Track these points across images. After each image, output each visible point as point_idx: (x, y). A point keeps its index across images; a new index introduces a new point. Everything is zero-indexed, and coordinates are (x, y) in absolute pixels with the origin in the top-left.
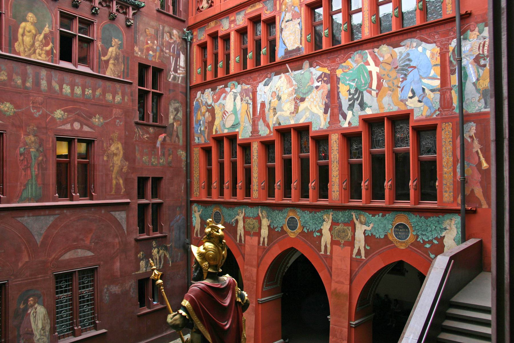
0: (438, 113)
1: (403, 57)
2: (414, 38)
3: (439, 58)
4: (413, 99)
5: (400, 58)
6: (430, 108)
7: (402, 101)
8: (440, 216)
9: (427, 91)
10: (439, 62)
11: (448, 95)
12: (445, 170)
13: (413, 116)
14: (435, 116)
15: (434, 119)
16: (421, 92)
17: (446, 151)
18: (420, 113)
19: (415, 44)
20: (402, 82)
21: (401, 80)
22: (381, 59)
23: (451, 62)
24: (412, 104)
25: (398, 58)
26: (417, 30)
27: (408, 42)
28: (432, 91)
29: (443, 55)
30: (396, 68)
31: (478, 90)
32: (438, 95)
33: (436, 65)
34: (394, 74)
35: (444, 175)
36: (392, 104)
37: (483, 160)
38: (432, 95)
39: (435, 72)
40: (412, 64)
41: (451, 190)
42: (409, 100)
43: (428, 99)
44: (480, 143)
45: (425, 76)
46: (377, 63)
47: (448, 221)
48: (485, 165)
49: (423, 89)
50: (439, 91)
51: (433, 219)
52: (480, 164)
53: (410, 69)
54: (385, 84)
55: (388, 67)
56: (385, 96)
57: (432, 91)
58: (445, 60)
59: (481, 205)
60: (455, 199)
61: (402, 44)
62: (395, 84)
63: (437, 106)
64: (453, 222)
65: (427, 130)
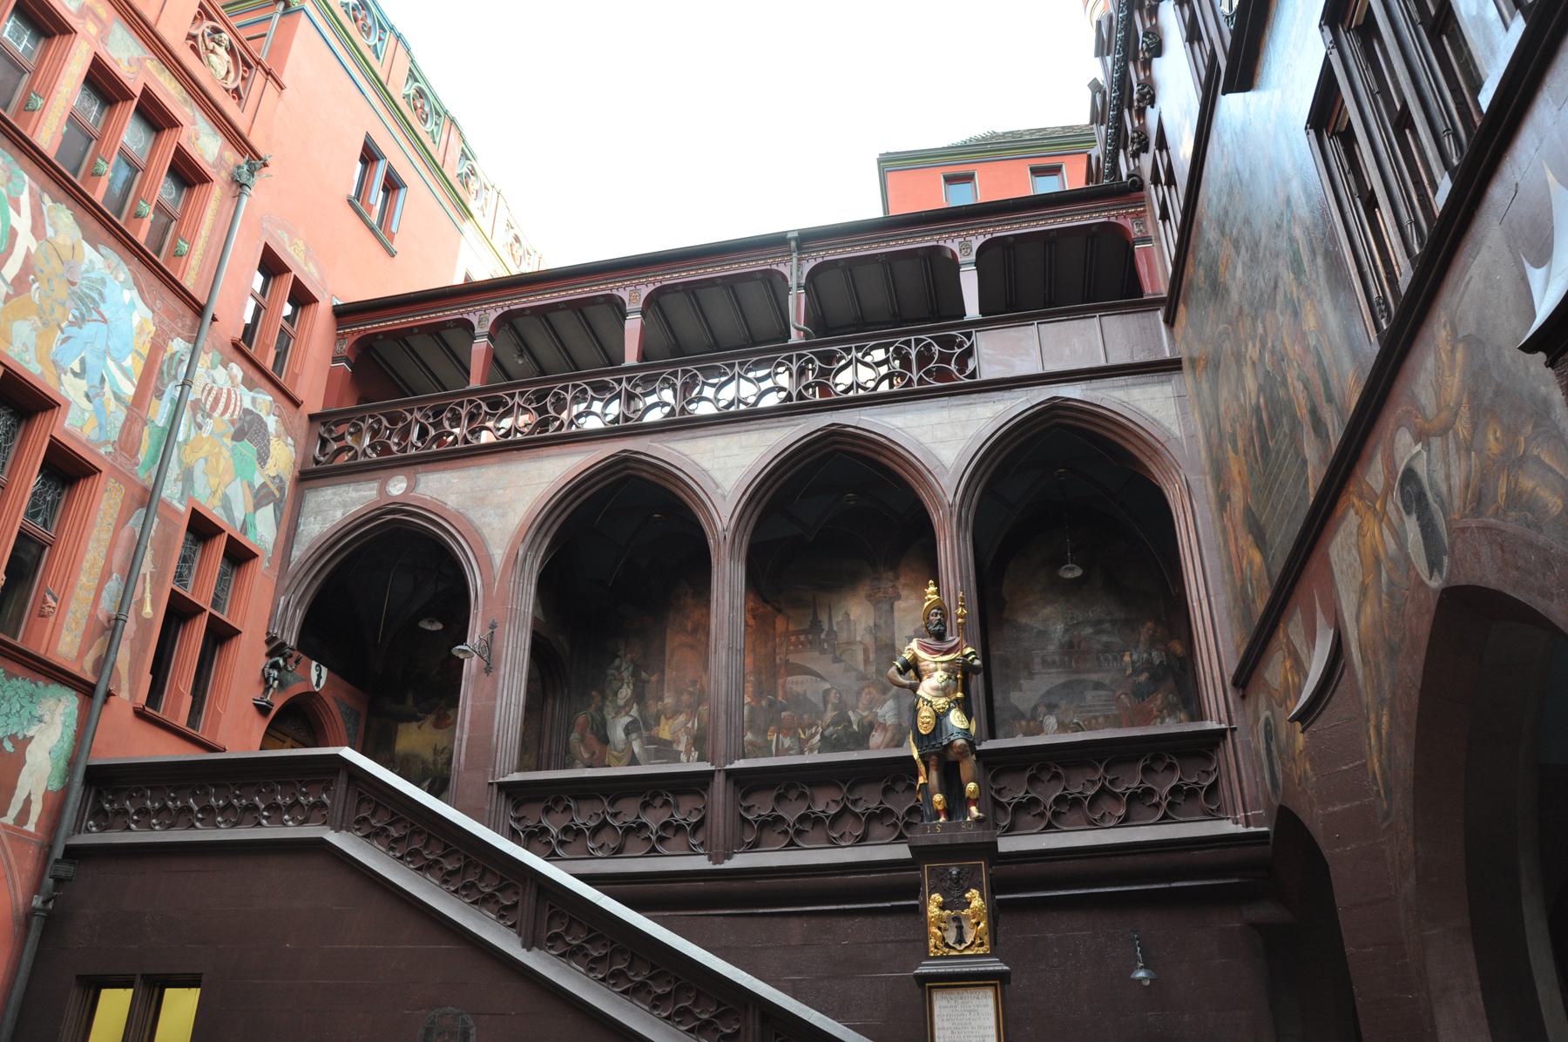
0: (110, 449)
1: (92, 275)
2: (127, 264)
3: (148, 346)
4: (77, 380)
5: (87, 271)
6: (101, 427)
7: (54, 363)
8: (40, 683)
9: (107, 385)
10: (145, 351)
11: (136, 428)
12: (83, 579)
13: (65, 417)
14: (102, 451)
15: (99, 455)
16: (97, 382)
17: (98, 540)
18: (80, 424)
19: (122, 277)
20: (71, 324)
21: (71, 317)
22: (50, 232)
23: (161, 372)
24: (70, 389)
25: (84, 267)
26: (136, 255)
27: (115, 258)
28: (117, 397)
29: (157, 347)
30: (73, 284)
31: (180, 461)
32: (121, 415)
33: (140, 354)
34: (62, 291)
35: (77, 590)
36: (32, 349)
37: (148, 596)
38: (113, 403)
39: (134, 364)
40: (103, 308)
41: (79, 632)
42: (70, 375)
43: (102, 404)
44: (154, 561)
45: (115, 354)
46: (37, 230)
47: (52, 702)
48: (148, 610)
49: (103, 380)
50: (128, 408)
51: (23, 685)
52: (141, 602)
53: (95, 316)
54: (35, 292)
55: (55, 263)
56: (25, 319)
57: (117, 397)
58: (155, 361)
59: (119, 688)
60: (81, 655)
61: (101, 248)
62: (58, 315)
63: (114, 435)
64: (61, 706)
65: (67, 470)
